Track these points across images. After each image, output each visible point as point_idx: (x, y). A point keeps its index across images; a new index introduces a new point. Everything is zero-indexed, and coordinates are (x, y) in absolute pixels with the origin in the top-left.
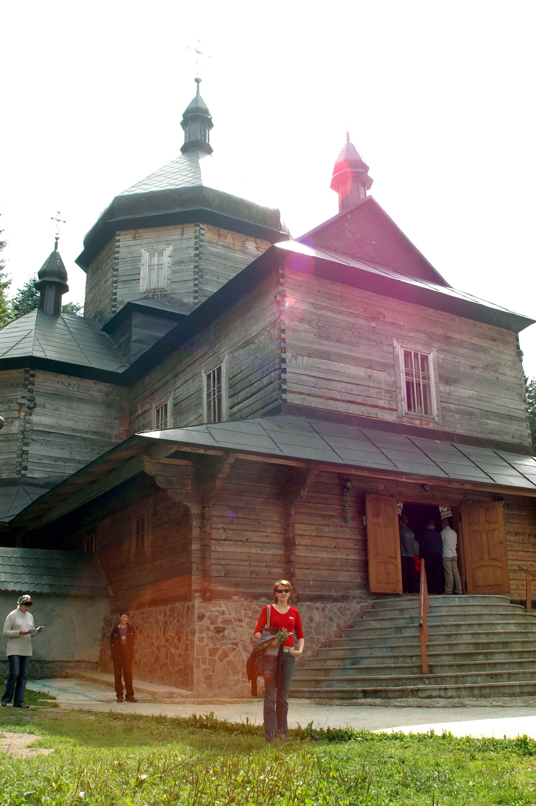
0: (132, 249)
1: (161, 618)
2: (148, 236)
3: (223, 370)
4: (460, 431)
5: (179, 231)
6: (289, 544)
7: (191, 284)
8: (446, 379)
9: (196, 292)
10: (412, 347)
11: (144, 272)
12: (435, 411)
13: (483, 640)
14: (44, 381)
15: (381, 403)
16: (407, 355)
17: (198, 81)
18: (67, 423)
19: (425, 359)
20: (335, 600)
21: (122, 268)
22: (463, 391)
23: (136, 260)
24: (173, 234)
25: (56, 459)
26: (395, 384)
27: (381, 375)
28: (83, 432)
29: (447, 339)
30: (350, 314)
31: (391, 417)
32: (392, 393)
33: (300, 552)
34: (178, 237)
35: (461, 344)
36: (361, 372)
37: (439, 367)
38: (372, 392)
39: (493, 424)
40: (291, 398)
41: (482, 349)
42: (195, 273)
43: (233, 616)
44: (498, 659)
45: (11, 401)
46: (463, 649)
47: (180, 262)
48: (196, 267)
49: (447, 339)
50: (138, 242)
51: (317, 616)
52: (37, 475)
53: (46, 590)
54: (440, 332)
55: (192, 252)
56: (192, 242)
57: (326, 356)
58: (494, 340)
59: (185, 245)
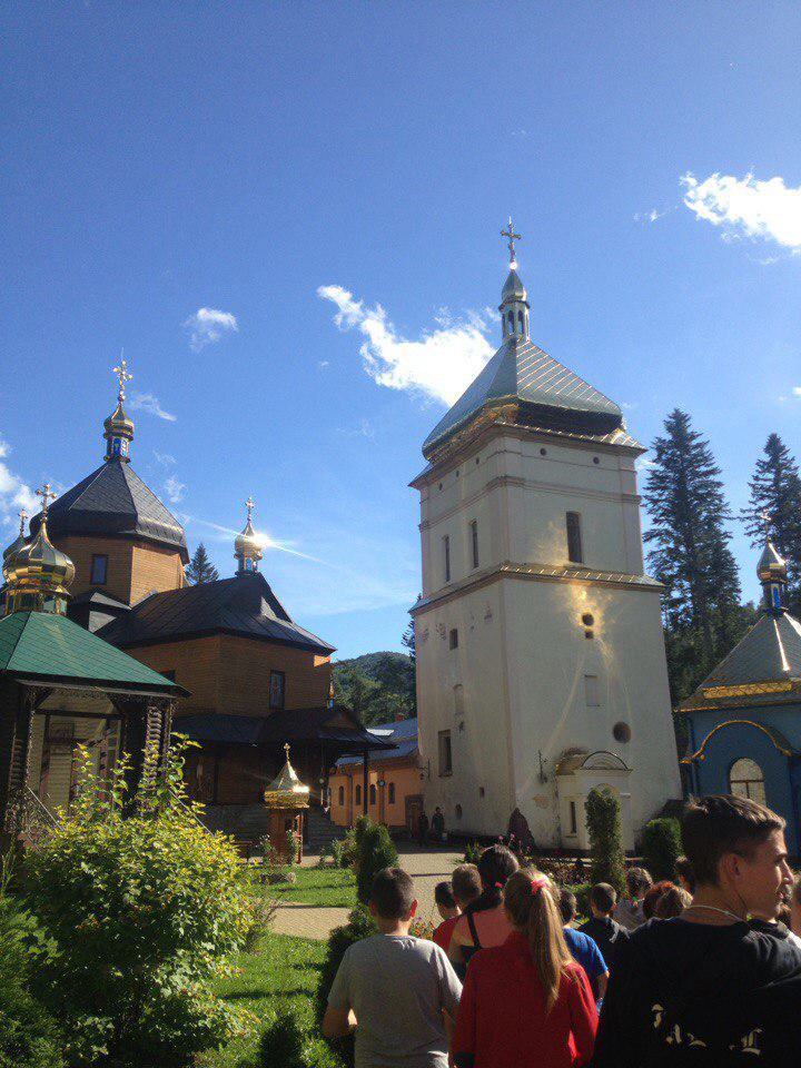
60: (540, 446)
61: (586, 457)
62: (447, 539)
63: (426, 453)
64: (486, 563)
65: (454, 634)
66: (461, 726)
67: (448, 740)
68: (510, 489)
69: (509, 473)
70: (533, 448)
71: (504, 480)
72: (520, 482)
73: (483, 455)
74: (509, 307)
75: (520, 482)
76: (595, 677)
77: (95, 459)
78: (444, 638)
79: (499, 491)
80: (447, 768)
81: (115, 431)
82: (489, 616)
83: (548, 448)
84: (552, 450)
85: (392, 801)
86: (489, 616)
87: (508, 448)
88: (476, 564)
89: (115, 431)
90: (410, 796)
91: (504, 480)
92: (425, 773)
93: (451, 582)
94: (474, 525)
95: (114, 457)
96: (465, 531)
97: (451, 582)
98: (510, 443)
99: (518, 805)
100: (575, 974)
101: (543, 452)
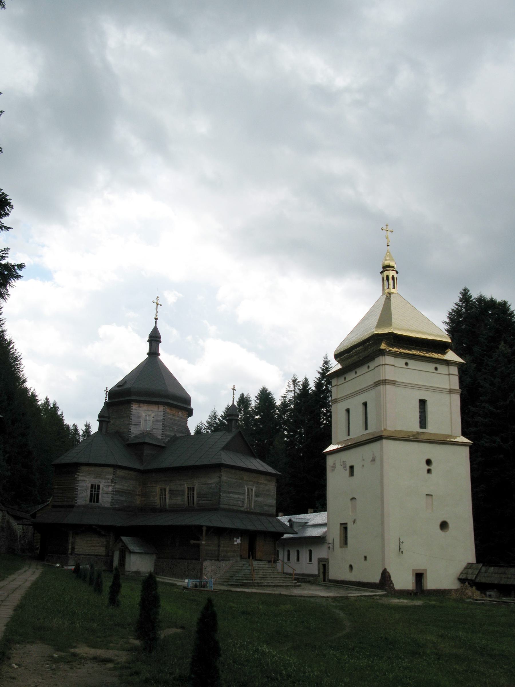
0: (138, 411)
1: (186, 564)
2: (145, 407)
3: (195, 489)
4: (258, 511)
5: (157, 407)
6: (219, 546)
7: (161, 431)
8: (257, 496)
9: (162, 434)
10: (250, 487)
11: (142, 422)
12: (253, 506)
13: (265, 574)
14: (120, 473)
15: (241, 505)
16: (248, 489)
17: (156, 319)
18: (125, 488)
19: (252, 490)
20: (226, 560)
21: (133, 419)
22: (260, 499)
23: (139, 416)
24: (155, 408)
25: (122, 501)
26: (244, 499)
27: (241, 497)
28: (129, 490)
29: (258, 483)
30: (236, 479)
31: (242, 509)
32: (243, 502)
33: (221, 549)
34: (156, 410)
35: (261, 484)
36: (236, 496)
37: (255, 492)
38: (239, 502)
39: (266, 508)
40: (222, 506)
41: (266, 485)
42: (163, 426)
43: (208, 565)
44: (269, 579)
45: (108, 479)
46: (260, 576)
47: (157, 421)
48: (163, 424)
49: (258, 483)
50: (140, 409)
51: (224, 565)
52: (117, 506)
53: (142, 551)
54: (256, 481)
55: (162, 418)
56: (162, 413)
57: (229, 493)
58: (269, 481)
59: (159, 413)
60: (404, 361)
62: (348, 411)
63: (337, 356)
65: (352, 467)
66: (354, 522)
67: (346, 529)
68: (388, 387)
70: (401, 362)
73: (372, 365)
74: (386, 273)
75: (393, 383)
76: (431, 495)
77: (140, 354)
78: (346, 470)
79: (381, 387)
80: (345, 542)
81: (155, 339)
82: (373, 460)
83: (409, 361)
84: (412, 364)
85: (310, 560)
86: (373, 460)
87: (387, 363)
89: (155, 339)
90: (321, 558)
91: (384, 382)
92: (330, 545)
94: (365, 404)
95: (153, 353)
96: (361, 408)
98: (388, 359)
99: (386, 567)
101: (406, 364)
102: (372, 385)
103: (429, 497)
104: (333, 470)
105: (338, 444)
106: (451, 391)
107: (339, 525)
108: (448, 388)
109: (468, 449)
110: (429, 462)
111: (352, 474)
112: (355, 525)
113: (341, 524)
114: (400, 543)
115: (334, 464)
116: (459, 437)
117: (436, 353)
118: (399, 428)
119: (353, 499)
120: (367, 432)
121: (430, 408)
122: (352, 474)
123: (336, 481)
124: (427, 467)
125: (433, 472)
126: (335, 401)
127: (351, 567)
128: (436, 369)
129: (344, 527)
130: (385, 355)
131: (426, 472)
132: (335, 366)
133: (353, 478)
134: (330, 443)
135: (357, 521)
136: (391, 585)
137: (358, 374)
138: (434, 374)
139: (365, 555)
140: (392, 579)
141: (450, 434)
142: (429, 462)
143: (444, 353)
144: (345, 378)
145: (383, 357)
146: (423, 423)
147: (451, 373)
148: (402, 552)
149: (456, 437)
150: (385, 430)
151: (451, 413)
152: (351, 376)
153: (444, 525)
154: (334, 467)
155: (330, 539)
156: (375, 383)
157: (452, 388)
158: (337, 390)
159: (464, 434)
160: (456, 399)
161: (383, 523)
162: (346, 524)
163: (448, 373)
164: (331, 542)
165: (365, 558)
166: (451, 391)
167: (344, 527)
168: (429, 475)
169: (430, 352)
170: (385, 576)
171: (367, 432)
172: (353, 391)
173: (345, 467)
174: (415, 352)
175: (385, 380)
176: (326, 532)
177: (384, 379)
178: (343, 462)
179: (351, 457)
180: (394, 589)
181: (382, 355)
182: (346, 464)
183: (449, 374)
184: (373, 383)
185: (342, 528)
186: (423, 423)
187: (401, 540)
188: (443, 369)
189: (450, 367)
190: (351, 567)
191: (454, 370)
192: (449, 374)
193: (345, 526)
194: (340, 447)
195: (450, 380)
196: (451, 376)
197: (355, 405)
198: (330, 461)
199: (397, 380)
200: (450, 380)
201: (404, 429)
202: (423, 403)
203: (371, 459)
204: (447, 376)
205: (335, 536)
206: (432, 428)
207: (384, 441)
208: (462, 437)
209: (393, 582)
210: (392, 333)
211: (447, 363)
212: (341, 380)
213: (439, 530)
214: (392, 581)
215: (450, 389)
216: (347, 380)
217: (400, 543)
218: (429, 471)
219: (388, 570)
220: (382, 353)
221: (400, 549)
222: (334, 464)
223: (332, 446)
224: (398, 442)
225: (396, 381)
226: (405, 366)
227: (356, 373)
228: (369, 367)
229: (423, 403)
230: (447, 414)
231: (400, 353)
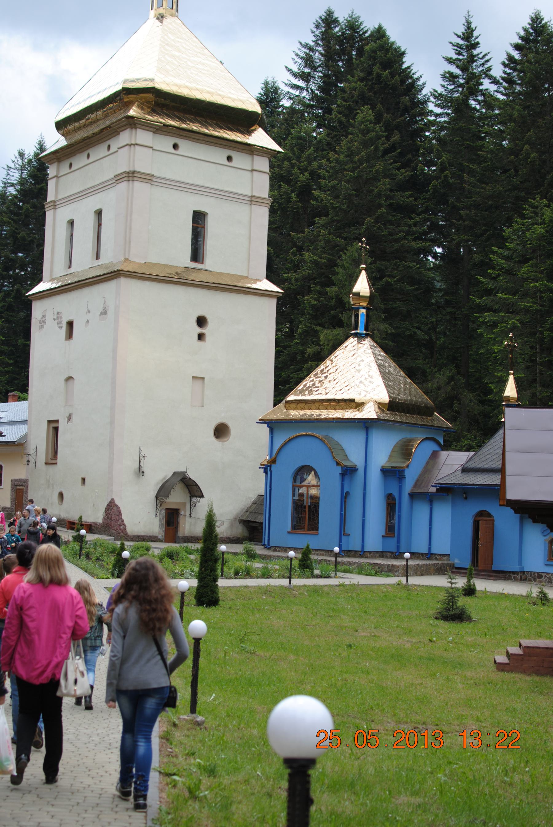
61: (219, 155)
62: (71, 223)
63: (60, 125)
64: (110, 257)
65: (70, 324)
66: (70, 418)
67: (56, 429)
68: (138, 185)
69: (137, 169)
70: (165, 143)
71: (131, 176)
72: (148, 178)
73: (115, 143)
75: (148, 178)
76: (203, 378)
78: (61, 328)
82: (104, 313)
84: (186, 146)
86: (104, 313)
87: (138, 142)
88: (98, 258)
90: (16, 480)
91: (131, 176)
93: (72, 270)
94: (99, 213)
97: (72, 270)
98: (143, 136)
100: (189, 648)
101: (175, 146)
102: (112, 179)
103: (199, 382)
104: (41, 327)
105: (52, 280)
106: (253, 200)
107: (46, 422)
108: (250, 195)
109: (274, 302)
110: (201, 321)
111: (70, 335)
112: (70, 423)
113: (49, 422)
114: (142, 457)
115: (44, 316)
116: (260, 281)
117: (231, 130)
118: (153, 259)
119: (70, 378)
120: (100, 262)
121: (212, 227)
122: (70, 335)
123: (45, 347)
124: (199, 330)
125: (208, 338)
126: (54, 205)
127: (61, 495)
128: (229, 159)
129: (54, 428)
130: (136, 128)
131: (196, 337)
132: (55, 141)
133: (71, 341)
134: (38, 279)
135: (74, 418)
136: (122, 527)
137: (91, 159)
138: (225, 168)
139: (83, 476)
140: (124, 517)
141: (245, 274)
142: (201, 321)
143: (248, 132)
144: (71, 165)
145: (134, 130)
146: (197, 254)
147: (255, 168)
148: (143, 472)
149: (256, 280)
150: (126, 260)
151: (250, 239)
152: (80, 161)
153: (221, 431)
154: (43, 322)
155: (31, 450)
156: (115, 176)
157: (255, 194)
158: (59, 185)
159: (271, 276)
160: (262, 216)
161: (112, 423)
162: (57, 421)
163: (250, 169)
164: (32, 452)
165: (84, 480)
166: (253, 200)
167: (54, 428)
168: (200, 343)
169: (221, 128)
170: (112, 510)
171: (100, 262)
172: (82, 189)
173: (59, 323)
174: (195, 127)
175: (134, 172)
176: (26, 436)
177: (132, 169)
178: (58, 313)
179: (69, 306)
180: (126, 534)
181: (132, 128)
182: (61, 317)
183: (253, 170)
184: (112, 176)
185: (51, 429)
186: (197, 254)
187: (143, 454)
188: (241, 160)
189: (255, 157)
190: (61, 495)
191: (263, 164)
192: (253, 170)
193: (55, 425)
194: (54, 286)
195: (252, 181)
196: (255, 173)
197: (83, 212)
198: (38, 310)
199: (156, 174)
200: (252, 181)
201: (163, 261)
202: (199, 218)
203: (101, 310)
204: (248, 174)
205: (39, 442)
206: (215, 261)
207: (123, 281)
208: (266, 281)
209: (125, 522)
210: (153, 88)
211: (251, 150)
212: (64, 168)
213: (213, 438)
214: (123, 521)
215: (252, 197)
216: (73, 168)
217: (142, 457)
218: (201, 337)
219: (117, 502)
220: (132, 123)
221: (140, 468)
222: (44, 316)
223: (41, 284)
224: (148, 283)
225: (152, 175)
226: (173, 151)
227: (88, 156)
228: (109, 147)
229: (199, 218)
230: (242, 240)
231: (165, 125)
